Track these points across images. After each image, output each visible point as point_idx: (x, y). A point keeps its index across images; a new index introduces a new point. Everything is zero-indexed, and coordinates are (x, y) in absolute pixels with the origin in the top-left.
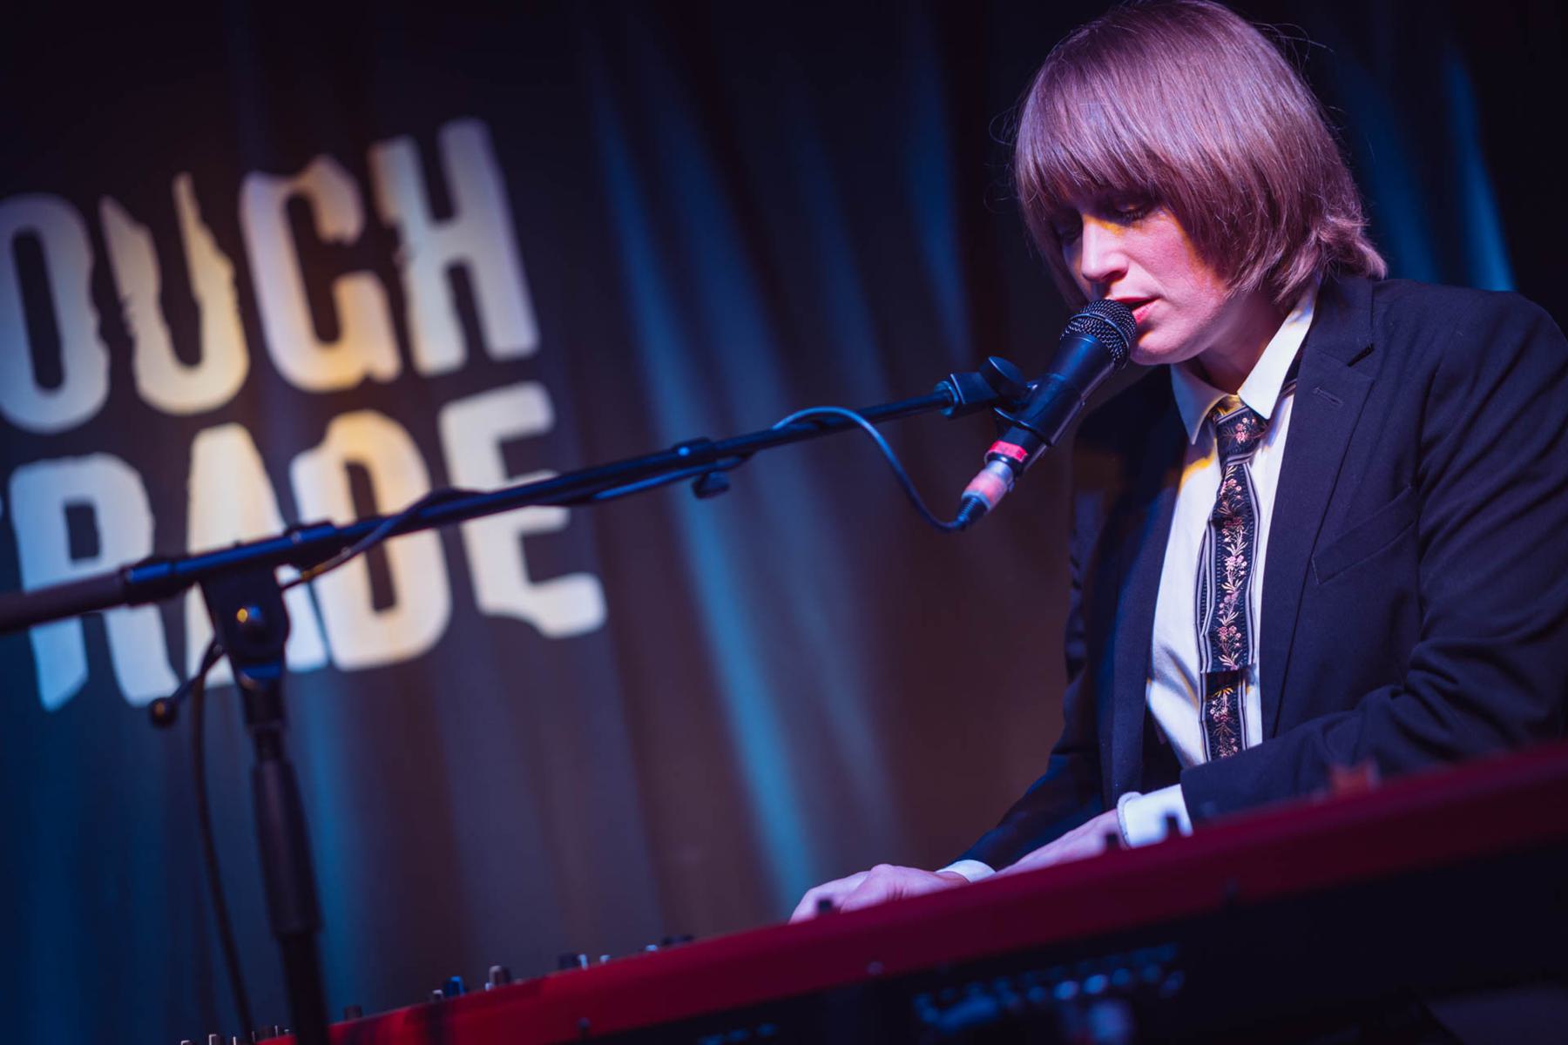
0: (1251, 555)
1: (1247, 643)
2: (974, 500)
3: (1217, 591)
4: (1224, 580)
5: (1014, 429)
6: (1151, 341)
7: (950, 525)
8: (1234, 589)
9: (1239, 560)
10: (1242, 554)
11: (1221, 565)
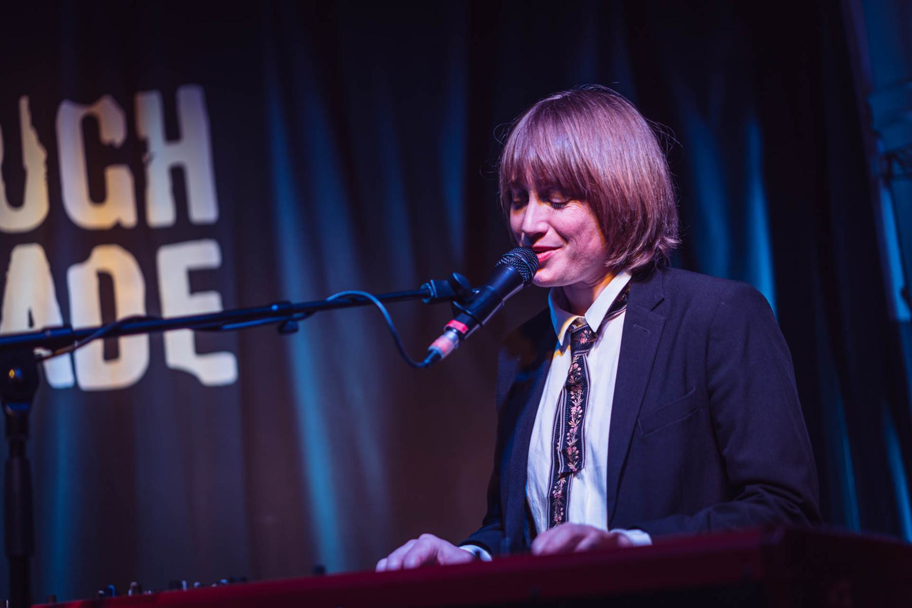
0: (585, 406)
1: (581, 456)
2: (435, 352)
3: (566, 425)
4: (570, 419)
5: (463, 314)
6: (544, 275)
7: (420, 364)
8: (575, 425)
9: (578, 409)
10: (580, 405)
11: (569, 411)
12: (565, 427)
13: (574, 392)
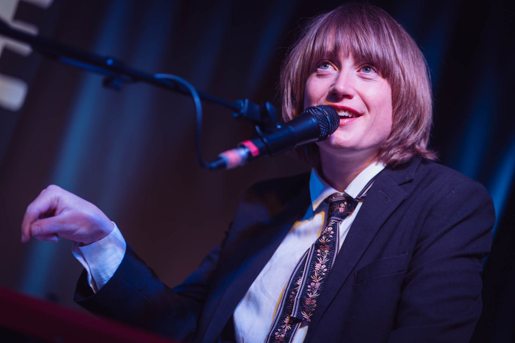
3: (308, 277)
4: (313, 274)
12: (307, 280)
13: (322, 251)
